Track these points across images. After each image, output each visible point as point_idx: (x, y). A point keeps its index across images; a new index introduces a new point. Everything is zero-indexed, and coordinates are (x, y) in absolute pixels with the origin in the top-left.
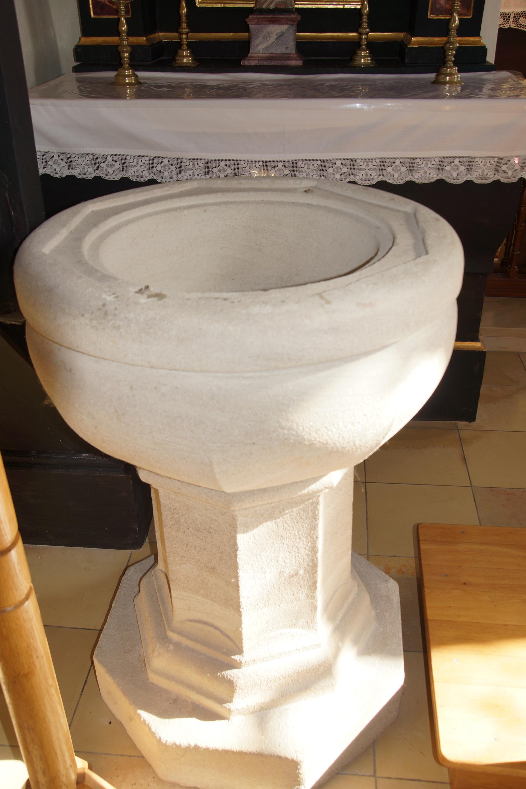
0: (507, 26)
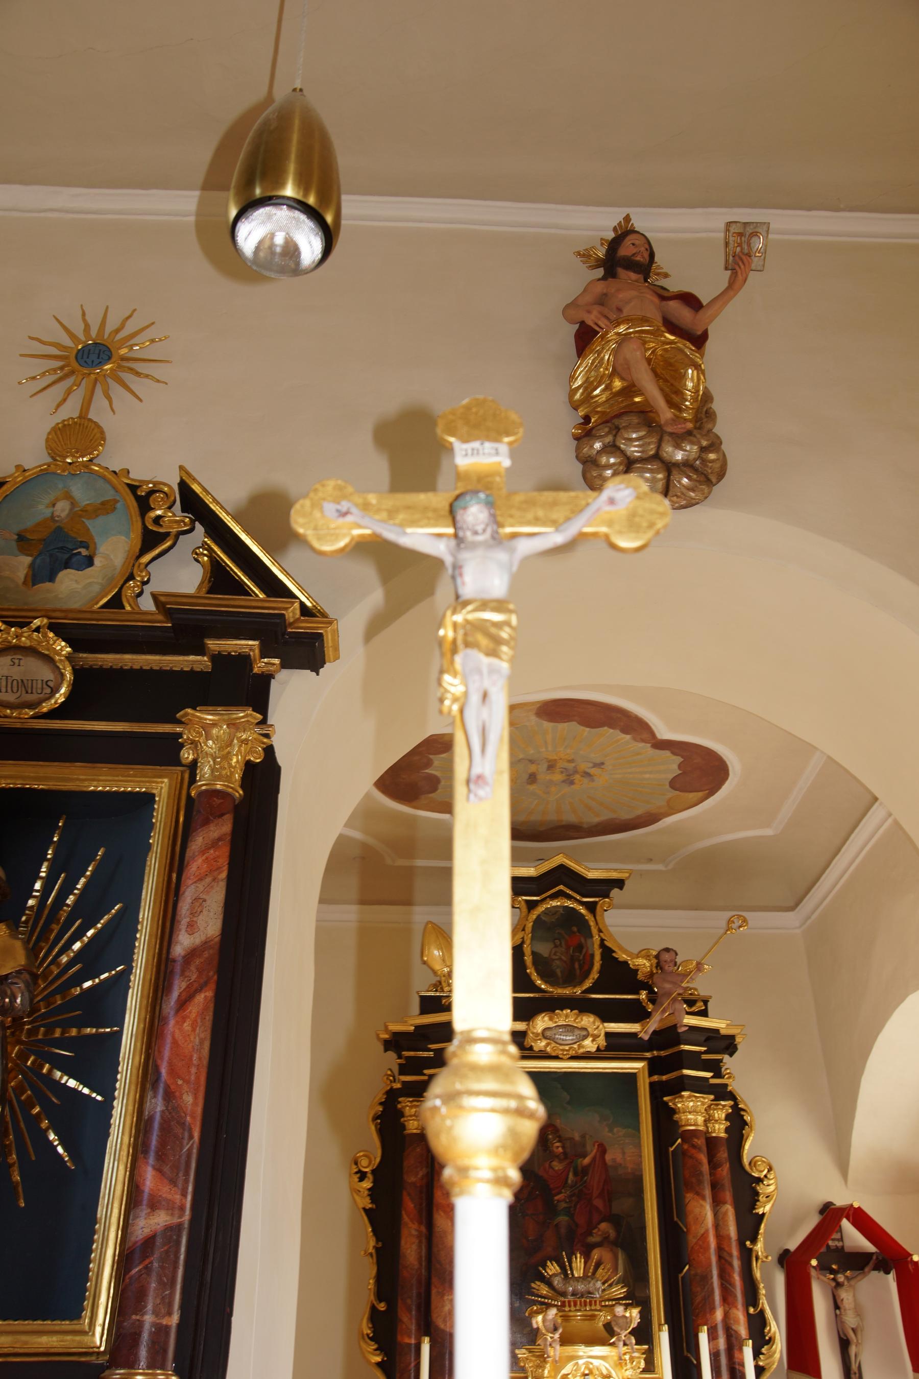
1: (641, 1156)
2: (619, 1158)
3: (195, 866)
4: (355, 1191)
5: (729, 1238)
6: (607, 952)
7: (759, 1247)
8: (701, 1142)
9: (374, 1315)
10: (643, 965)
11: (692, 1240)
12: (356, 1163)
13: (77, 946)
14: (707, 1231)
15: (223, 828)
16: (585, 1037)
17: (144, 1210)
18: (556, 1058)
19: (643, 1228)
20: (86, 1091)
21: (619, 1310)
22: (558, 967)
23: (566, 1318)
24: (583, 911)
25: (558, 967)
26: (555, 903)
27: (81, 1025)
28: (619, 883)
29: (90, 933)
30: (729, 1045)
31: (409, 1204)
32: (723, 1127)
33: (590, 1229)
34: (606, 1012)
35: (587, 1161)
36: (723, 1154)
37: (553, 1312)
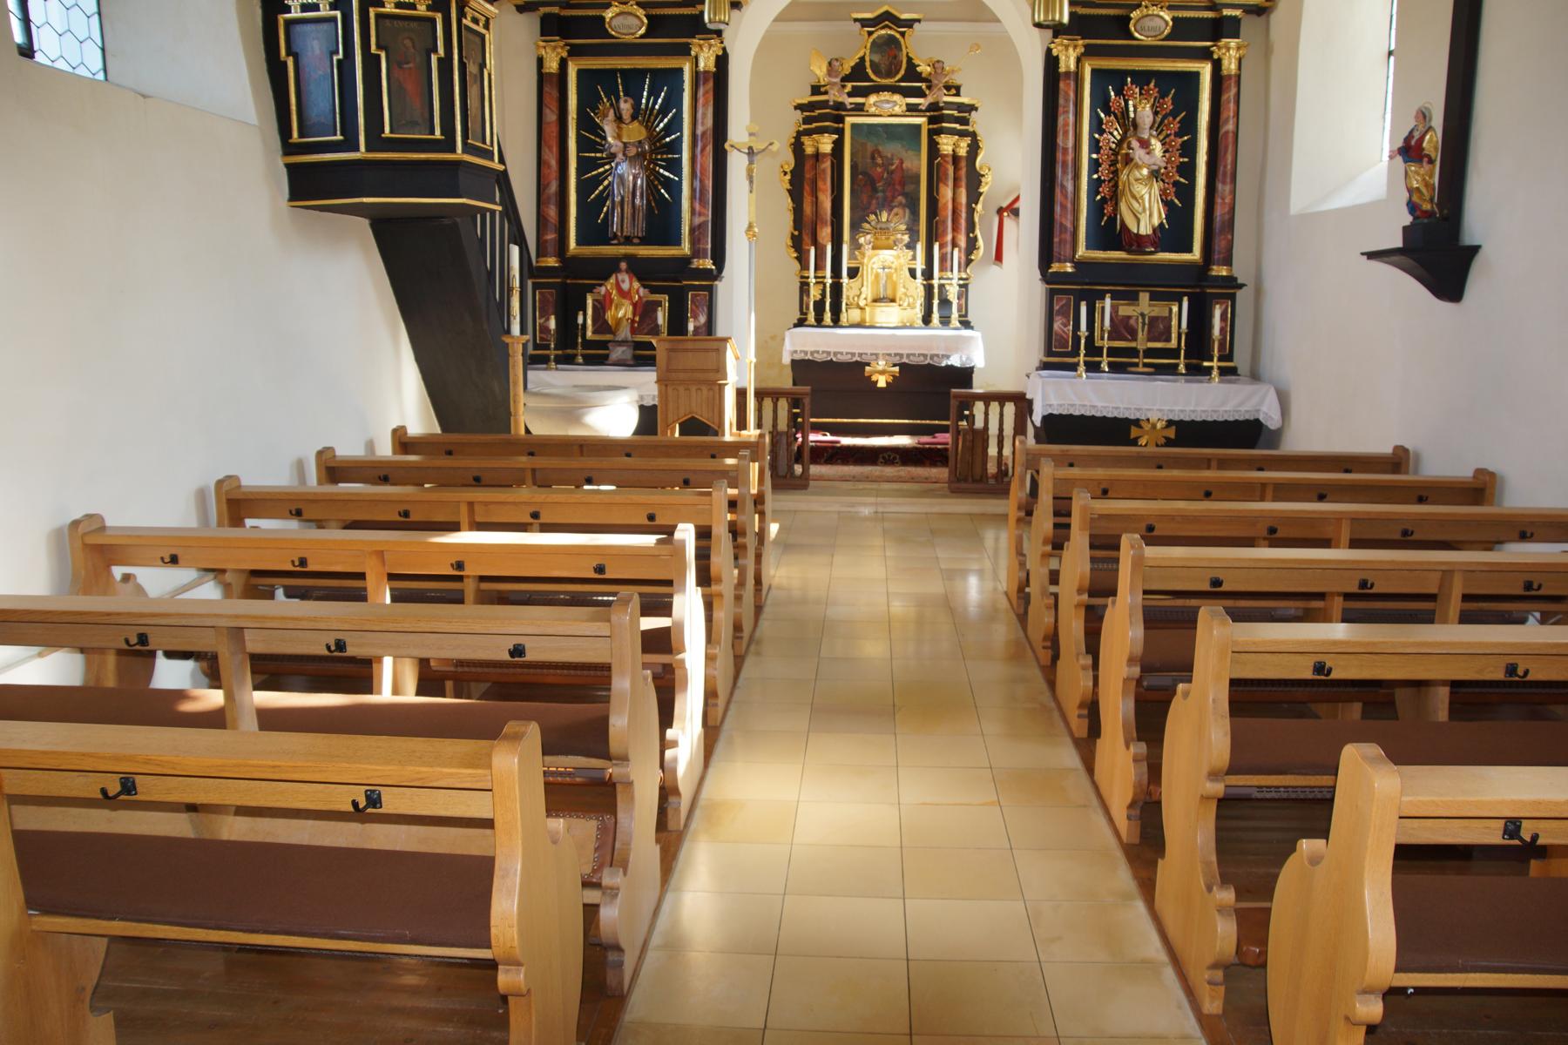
0: (807, 358)
1: (920, 165)
2: (909, 166)
3: (701, 101)
4: (782, 181)
5: (961, 204)
6: (909, 60)
7: (979, 207)
8: (950, 159)
9: (792, 234)
10: (924, 69)
11: (940, 205)
12: (782, 167)
13: (662, 125)
14: (947, 202)
15: (710, 84)
16: (895, 106)
17: (697, 216)
18: (881, 116)
19: (919, 199)
20: (672, 176)
21: (899, 236)
22: (883, 68)
23: (877, 239)
24: (898, 36)
25: (883, 68)
26: (883, 32)
27: (667, 154)
28: (919, 21)
29: (660, 101)
30: (972, 108)
31: (807, 188)
32: (965, 151)
33: (894, 197)
34: (906, 93)
35: (894, 167)
36: (963, 164)
37: (869, 237)
